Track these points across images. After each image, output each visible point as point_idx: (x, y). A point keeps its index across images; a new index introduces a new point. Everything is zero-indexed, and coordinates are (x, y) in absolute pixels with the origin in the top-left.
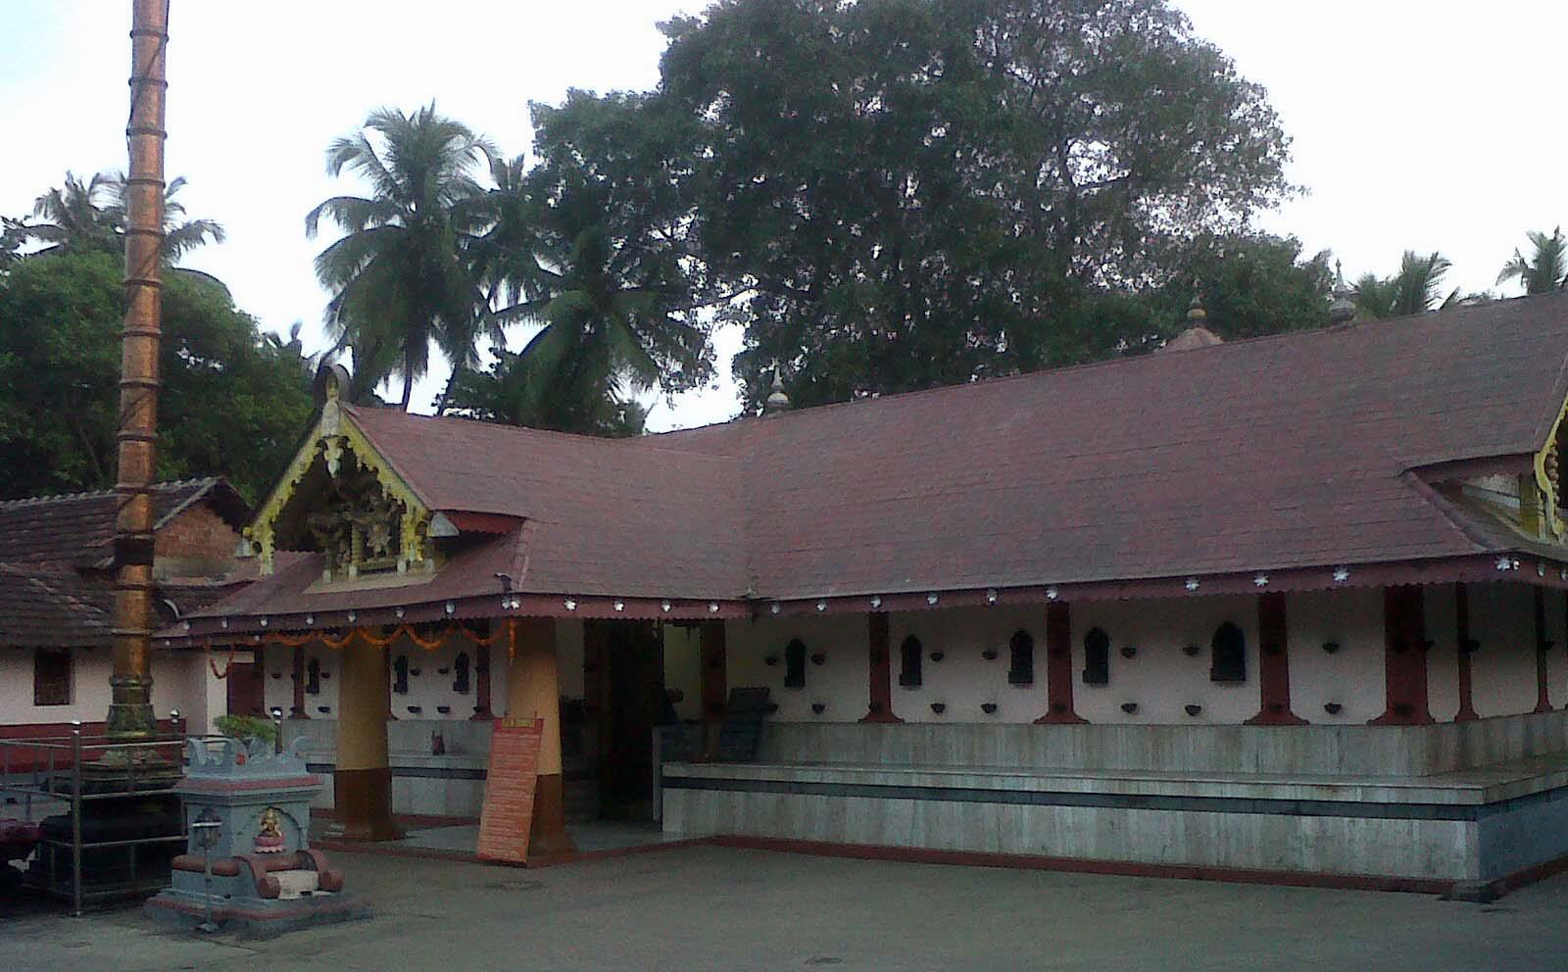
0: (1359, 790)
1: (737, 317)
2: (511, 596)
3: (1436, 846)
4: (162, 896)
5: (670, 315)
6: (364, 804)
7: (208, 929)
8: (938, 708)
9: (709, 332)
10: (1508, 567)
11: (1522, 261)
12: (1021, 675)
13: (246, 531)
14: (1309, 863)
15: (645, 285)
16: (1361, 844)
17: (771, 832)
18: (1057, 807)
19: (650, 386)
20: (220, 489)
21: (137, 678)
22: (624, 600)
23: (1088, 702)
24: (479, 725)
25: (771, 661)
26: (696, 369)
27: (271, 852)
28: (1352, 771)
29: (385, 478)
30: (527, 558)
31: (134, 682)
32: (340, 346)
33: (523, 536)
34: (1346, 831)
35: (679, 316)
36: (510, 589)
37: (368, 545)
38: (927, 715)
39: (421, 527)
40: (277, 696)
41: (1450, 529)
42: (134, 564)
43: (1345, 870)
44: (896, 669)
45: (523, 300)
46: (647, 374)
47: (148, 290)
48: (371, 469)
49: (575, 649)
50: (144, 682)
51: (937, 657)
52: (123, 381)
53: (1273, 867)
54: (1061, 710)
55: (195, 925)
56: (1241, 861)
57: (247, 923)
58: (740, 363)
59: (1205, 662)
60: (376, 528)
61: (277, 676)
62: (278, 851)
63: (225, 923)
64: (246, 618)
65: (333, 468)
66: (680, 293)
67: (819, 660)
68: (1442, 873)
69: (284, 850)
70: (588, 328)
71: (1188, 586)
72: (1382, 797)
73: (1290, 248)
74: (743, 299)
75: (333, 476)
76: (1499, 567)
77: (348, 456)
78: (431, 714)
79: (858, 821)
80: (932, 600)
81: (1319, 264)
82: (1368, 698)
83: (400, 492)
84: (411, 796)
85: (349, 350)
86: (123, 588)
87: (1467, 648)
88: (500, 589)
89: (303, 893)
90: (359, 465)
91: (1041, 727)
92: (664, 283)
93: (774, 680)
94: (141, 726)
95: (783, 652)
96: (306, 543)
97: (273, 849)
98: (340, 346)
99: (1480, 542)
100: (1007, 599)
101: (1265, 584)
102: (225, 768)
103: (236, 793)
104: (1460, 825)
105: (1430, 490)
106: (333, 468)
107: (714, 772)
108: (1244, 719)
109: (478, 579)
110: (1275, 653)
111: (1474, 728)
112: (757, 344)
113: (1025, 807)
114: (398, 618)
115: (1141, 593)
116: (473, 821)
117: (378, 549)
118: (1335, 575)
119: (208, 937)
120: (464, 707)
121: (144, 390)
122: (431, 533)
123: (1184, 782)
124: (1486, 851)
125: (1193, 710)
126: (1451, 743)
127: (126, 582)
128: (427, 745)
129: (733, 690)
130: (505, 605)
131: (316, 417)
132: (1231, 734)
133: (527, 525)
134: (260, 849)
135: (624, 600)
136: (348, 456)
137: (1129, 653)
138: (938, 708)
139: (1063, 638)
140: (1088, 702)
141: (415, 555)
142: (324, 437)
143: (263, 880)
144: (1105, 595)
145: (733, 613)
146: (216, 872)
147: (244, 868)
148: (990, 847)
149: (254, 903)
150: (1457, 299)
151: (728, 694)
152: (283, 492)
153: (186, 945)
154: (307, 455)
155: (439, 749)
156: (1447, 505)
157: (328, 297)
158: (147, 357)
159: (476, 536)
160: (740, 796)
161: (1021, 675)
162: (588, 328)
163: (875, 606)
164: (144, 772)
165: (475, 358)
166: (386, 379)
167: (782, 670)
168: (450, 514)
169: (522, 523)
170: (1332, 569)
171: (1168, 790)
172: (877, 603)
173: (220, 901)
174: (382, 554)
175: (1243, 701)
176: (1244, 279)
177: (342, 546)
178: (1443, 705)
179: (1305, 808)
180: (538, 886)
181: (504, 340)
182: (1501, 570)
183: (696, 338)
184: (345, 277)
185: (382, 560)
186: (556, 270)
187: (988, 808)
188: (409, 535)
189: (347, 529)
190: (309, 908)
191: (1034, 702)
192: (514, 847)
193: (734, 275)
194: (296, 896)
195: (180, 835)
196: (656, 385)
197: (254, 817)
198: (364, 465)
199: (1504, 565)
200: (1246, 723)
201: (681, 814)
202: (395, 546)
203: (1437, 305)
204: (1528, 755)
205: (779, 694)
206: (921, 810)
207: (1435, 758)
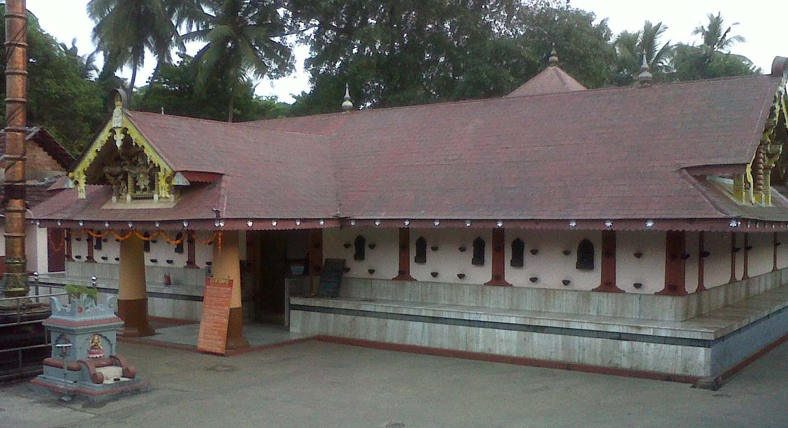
0: (652, 330)
1: (306, 40)
2: (220, 220)
3: (690, 359)
4: (39, 378)
5: (272, 39)
6: (135, 316)
7: (66, 400)
8: (435, 275)
9: (293, 48)
10: (736, 225)
11: (702, 27)
12: (478, 260)
13: (71, 174)
14: (625, 364)
15: (260, 24)
16: (652, 356)
17: (347, 335)
18: (497, 330)
19: (262, 77)
20: (42, 133)
21: (19, 259)
22: (277, 220)
23: (512, 275)
24: (189, 271)
25: (347, 246)
26: (285, 66)
27: (97, 357)
28: (644, 318)
29: (149, 152)
30: (226, 197)
31: (18, 261)
32: (97, 50)
33: (223, 185)
34: (644, 349)
35: (277, 39)
36: (220, 217)
37: (137, 184)
38: (428, 277)
39: (169, 180)
40: (79, 249)
41: (705, 202)
42: (17, 199)
43: (643, 368)
44: (413, 254)
45: (194, 29)
46: (262, 70)
47: (20, 49)
48: (140, 146)
49: (243, 239)
50: (23, 261)
51: (435, 249)
52: (7, 99)
53: (606, 364)
54: (498, 279)
55: (60, 398)
56: (590, 360)
57: (87, 397)
58: (308, 62)
59: (574, 258)
60: (141, 176)
61: (78, 240)
62: (100, 357)
63: (75, 396)
64: (68, 221)
65: (119, 144)
66: (278, 27)
67: (372, 246)
68: (692, 372)
69: (103, 356)
70: (230, 44)
71: (571, 224)
72: (663, 334)
73: (589, 18)
74: (310, 32)
75: (119, 148)
76: (731, 225)
77: (127, 140)
78: (162, 263)
79: (393, 331)
80: (437, 223)
81: (603, 25)
82: (656, 281)
83: (157, 160)
84: (158, 308)
85: (102, 53)
86: (11, 211)
87: (703, 254)
88: (215, 217)
89: (115, 380)
90: (134, 144)
91: (488, 288)
92: (270, 22)
93: (348, 255)
94: (22, 285)
95: (354, 242)
96: (103, 180)
97: (98, 356)
98: (97, 50)
99: (721, 211)
100: (476, 225)
101: (611, 226)
102: (72, 314)
103: (78, 328)
104: (702, 349)
105: (693, 179)
106: (119, 144)
107: (317, 303)
108: (592, 288)
109: (199, 209)
110: (610, 255)
111: (705, 293)
112: (316, 54)
113: (480, 328)
114: (157, 227)
115: (545, 226)
116: (191, 322)
117: (143, 187)
118: (646, 223)
119: (65, 404)
120: (181, 261)
121: (19, 104)
122: (174, 183)
123: (563, 321)
124: (715, 361)
125: (566, 283)
126: (694, 303)
127: (11, 208)
128: (161, 280)
129: (326, 260)
130: (217, 225)
131: (109, 116)
132: (585, 295)
133: (224, 178)
134: (91, 356)
135: (277, 220)
136: (127, 140)
137: (534, 252)
138: (435, 275)
139: (501, 245)
140: (512, 275)
141: (165, 194)
142: (114, 127)
143: (95, 374)
144: (527, 226)
145: (332, 225)
146: (70, 369)
147: (84, 367)
148: (461, 348)
149: (89, 386)
150: (670, 45)
151: (324, 261)
152: (91, 155)
153: (58, 411)
154: (104, 136)
155: (168, 283)
156: (704, 189)
157: (92, 24)
158: (20, 87)
159: (199, 184)
160: (331, 316)
161: (478, 260)
162: (230, 44)
163: (406, 224)
164: (24, 310)
165: (169, 58)
166: (122, 67)
167: (352, 251)
168: (184, 172)
169: (222, 176)
170: (646, 220)
171: (555, 324)
172: (407, 223)
173: (72, 384)
174: (145, 190)
175: (592, 279)
176: (568, 34)
177: (123, 185)
178: (691, 286)
179: (623, 337)
180: (232, 369)
181: (185, 50)
182: (732, 226)
183: (286, 52)
184: (101, 15)
185: (145, 193)
186: (213, 14)
187: (462, 329)
188: (162, 183)
189: (126, 175)
190: (120, 389)
191: (484, 274)
192: (218, 346)
193: (307, 18)
194: (111, 382)
195: (44, 344)
196: (266, 77)
197: (88, 339)
198: (136, 144)
199: (733, 224)
200: (593, 290)
201: (300, 324)
202: (152, 185)
203: (659, 48)
204: (726, 305)
205: (351, 263)
206: (426, 330)
207: (687, 313)
